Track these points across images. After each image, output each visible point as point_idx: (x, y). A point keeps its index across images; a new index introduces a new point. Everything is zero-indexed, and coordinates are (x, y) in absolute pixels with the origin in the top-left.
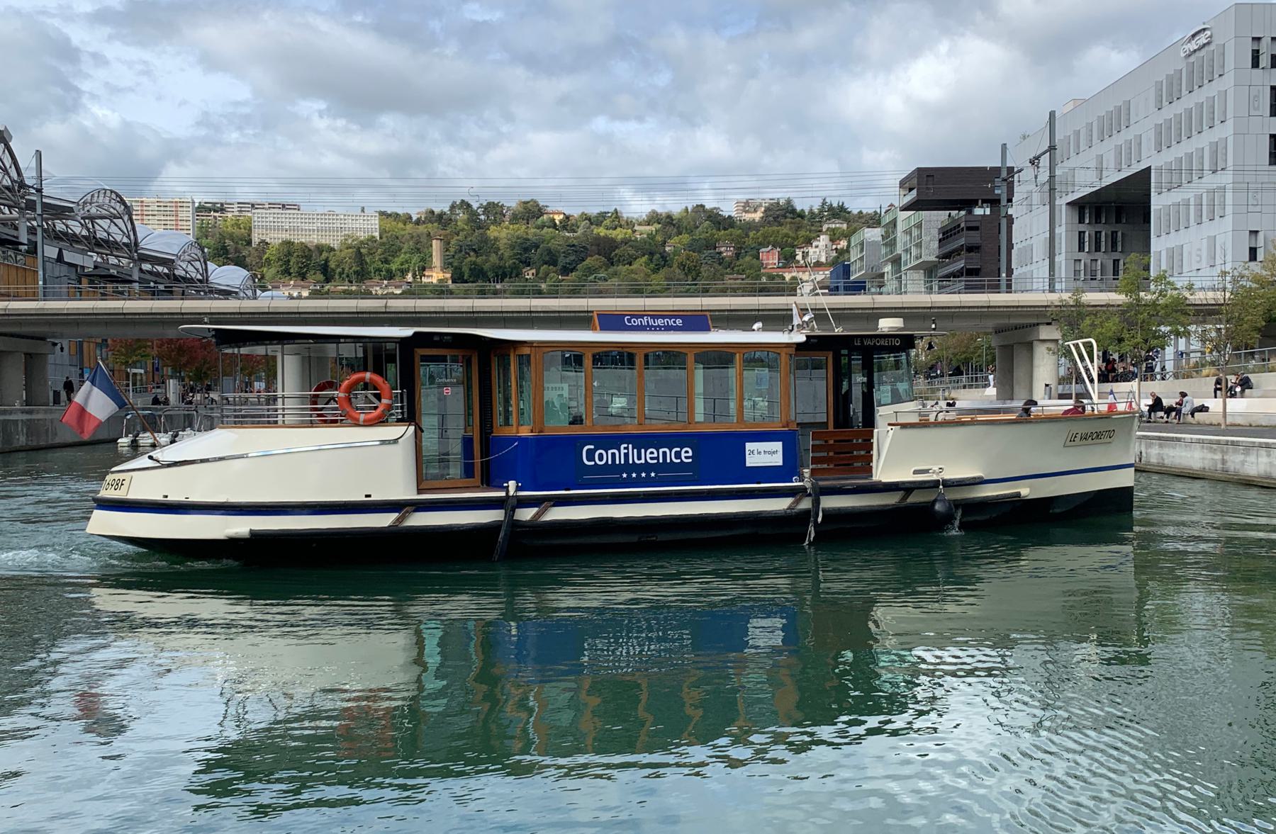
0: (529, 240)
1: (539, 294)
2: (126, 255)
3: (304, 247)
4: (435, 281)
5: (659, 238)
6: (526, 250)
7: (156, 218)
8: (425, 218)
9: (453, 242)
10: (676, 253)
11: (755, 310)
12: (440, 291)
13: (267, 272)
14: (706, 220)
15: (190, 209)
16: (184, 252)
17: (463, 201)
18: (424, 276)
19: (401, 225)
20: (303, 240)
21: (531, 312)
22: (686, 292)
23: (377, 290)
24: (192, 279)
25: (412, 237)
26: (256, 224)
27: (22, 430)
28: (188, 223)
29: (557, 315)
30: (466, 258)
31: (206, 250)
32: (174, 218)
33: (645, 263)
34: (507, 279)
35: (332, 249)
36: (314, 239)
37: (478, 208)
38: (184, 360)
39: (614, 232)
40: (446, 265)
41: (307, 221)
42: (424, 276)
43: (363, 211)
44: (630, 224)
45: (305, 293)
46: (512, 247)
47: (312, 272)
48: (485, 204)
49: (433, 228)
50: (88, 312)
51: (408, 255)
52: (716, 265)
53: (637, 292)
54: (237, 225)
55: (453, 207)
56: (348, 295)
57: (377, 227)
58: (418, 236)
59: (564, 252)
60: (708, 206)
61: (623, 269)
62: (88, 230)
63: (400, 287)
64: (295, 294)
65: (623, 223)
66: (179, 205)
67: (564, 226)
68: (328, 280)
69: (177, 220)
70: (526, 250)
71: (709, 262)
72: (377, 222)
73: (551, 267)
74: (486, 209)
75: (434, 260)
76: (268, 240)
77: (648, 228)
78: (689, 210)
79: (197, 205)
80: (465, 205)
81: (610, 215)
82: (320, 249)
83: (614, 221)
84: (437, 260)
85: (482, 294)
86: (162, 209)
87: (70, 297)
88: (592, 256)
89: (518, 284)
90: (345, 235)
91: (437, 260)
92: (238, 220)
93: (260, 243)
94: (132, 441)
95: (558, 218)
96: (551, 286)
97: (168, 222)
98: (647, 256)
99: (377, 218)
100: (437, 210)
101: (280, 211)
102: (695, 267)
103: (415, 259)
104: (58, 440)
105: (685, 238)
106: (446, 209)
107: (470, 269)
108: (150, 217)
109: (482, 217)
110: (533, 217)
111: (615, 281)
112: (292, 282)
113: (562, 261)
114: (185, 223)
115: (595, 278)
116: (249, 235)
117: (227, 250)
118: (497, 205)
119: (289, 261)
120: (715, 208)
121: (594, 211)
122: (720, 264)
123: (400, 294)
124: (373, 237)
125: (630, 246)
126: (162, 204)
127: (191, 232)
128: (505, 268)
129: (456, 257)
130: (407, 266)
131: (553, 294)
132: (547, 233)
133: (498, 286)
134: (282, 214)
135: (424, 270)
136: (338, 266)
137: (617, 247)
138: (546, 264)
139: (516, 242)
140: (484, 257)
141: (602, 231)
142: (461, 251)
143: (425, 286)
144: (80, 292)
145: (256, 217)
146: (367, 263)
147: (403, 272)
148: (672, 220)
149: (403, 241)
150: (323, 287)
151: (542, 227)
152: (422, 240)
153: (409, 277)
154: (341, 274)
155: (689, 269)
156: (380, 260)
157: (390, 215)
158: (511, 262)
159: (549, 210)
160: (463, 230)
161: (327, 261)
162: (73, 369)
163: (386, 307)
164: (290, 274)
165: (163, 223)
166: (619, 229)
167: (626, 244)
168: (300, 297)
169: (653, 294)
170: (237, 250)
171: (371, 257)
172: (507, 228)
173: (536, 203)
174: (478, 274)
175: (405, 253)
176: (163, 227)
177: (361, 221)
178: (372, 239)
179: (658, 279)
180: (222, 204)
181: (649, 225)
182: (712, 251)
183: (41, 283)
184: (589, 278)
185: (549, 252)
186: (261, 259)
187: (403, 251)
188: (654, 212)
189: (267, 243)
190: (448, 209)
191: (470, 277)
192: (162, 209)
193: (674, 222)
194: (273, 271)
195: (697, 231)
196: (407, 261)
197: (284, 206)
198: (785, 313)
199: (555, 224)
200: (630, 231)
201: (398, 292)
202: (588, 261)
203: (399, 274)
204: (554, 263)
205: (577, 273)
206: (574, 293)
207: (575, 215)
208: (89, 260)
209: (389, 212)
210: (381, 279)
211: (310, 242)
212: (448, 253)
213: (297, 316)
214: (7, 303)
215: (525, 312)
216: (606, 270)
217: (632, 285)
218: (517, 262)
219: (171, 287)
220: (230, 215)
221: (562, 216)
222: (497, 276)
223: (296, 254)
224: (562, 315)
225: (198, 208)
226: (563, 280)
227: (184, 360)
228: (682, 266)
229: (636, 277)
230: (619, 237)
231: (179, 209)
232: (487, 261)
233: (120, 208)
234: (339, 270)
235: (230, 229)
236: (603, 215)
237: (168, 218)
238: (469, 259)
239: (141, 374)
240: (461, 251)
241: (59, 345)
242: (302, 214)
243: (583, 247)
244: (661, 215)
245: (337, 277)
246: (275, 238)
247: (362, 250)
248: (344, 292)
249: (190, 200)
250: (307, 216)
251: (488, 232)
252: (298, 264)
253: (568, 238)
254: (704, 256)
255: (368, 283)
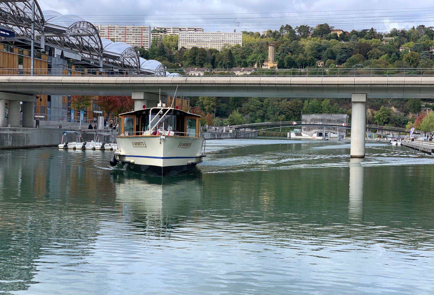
0: (321, 46)
1: (325, 74)
2: (97, 54)
3: (203, 50)
4: (269, 68)
5: (396, 44)
6: (319, 51)
7: (132, 36)
8: (267, 35)
9: (280, 47)
10: (406, 52)
11: (386, 84)
12: (272, 73)
13: (184, 63)
14: (425, 34)
15: (149, 31)
16: (125, 53)
17: (287, 25)
18: (263, 65)
19: (253, 39)
20: (203, 47)
21: (260, 84)
22: (409, 74)
23: (238, 73)
24: (132, 66)
25: (259, 45)
26: (180, 39)
27: (10, 138)
28: (147, 38)
29: (274, 86)
30: (285, 56)
31: (138, 52)
32: (140, 36)
33: (386, 58)
34: (307, 67)
35: (217, 51)
36: (209, 46)
37: (295, 29)
38: (110, 107)
39: (370, 41)
40: (276, 59)
41: (206, 37)
42: (263, 65)
43: (235, 32)
44: (380, 36)
45: (202, 74)
46: (312, 49)
47: (206, 63)
48: (299, 27)
49: (269, 40)
50: (46, 82)
51: (256, 54)
52: (429, 60)
53: (380, 73)
54: (171, 39)
55: (282, 29)
56: (222, 75)
57: (241, 39)
58: (262, 44)
59: (340, 52)
60: (427, 26)
61: (372, 61)
62: (79, 42)
63: (250, 70)
64: (197, 74)
65: (376, 36)
66: (143, 29)
67: (342, 38)
68: (214, 67)
69: (142, 37)
70: (319, 51)
71: (425, 57)
72: (241, 37)
73: (332, 60)
74: (299, 29)
75: (269, 57)
76: (186, 47)
77: (390, 38)
78: (415, 28)
79: (152, 29)
80: (288, 27)
81: (369, 31)
82: (212, 51)
83: (371, 34)
84: (271, 57)
85: (294, 74)
86: (135, 31)
87: (64, 74)
88: (356, 54)
89: (313, 69)
90: (225, 44)
91: (271, 57)
92: (172, 37)
93: (181, 48)
94: (65, 146)
95: (339, 33)
96: (332, 70)
97: (138, 38)
98: (387, 54)
99: (241, 35)
100: (273, 30)
101: (194, 32)
102: (416, 60)
103: (260, 56)
104: (30, 144)
105: (412, 44)
106: (278, 30)
107: (288, 62)
108: (129, 36)
109: (297, 34)
110: (325, 33)
111: (367, 68)
112: (196, 68)
113: (338, 57)
114: (146, 38)
115: (356, 66)
116: (177, 44)
117: (165, 52)
118: (306, 27)
119: (195, 57)
120: (431, 27)
121: (359, 28)
122: (431, 59)
123: (249, 74)
124: (239, 45)
125: (379, 49)
126: (135, 29)
127: (148, 43)
128: (307, 61)
129: (281, 55)
130: (255, 60)
131: (333, 74)
132: (332, 42)
133: (303, 70)
134: (194, 33)
135: (264, 62)
136: (219, 60)
137: (371, 49)
138: (329, 58)
139: (314, 47)
140: (296, 55)
141: (363, 40)
142: (284, 52)
143: (263, 70)
144: (71, 72)
145: (181, 35)
146: (234, 59)
147: (253, 64)
148: (405, 34)
149: (254, 46)
150: (211, 70)
151: (329, 39)
152: (264, 46)
153: (256, 66)
154: (221, 64)
155: (412, 61)
156: (241, 57)
157: (249, 33)
158: (310, 57)
159: (334, 29)
160: (286, 40)
161: (214, 57)
162: (64, 110)
163: (186, 81)
164: (195, 64)
165: (135, 38)
166: (373, 39)
167: (376, 47)
168: (199, 76)
169: (391, 74)
170: (171, 52)
171: (237, 55)
172: (310, 39)
173: (327, 25)
174: (292, 64)
175: (255, 53)
176: (135, 40)
177: (233, 37)
178: (238, 46)
179: (391, 67)
180: (165, 29)
181: (391, 37)
182: (427, 51)
183: (32, 67)
184: (353, 66)
185: (332, 52)
186: (182, 56)
187: (254, 52)
188: (395, 29)
189: (185, 49)
190: (279, 29)
191: (287, 65)
192: (135, 31)
193: (406, 35)
194: (187, 62)
195: (419, 40)
196: (255, 58)
197: (195, 29)
198: (403, 86)
199: (337, 37)
200: (379, 40)
201: (249, 73)
202: (353, 57)
203: (251, 64)
204: (334, 58)
205: (347, 63)
206: (344, 74)
207: (349, 32)
208: (78, 57)
209: (248, 32)
210: (241, 67)
211: (207, 48)
212: (277, 53)
213: (143, 85)
214: (9, 77)
215: (257, 84)
216: (363, 62)
217: (378, 70)
218: (313, 57)
219: (122, 70)
220: (168, 34)
221: (341, 32)
222: (302, 65)
223: (199, 54)
224: (277, 86)
225: (153, 31)
226: (338, 67)
227: (110, 107)
228: (408, 59)
229: (380, 65)
230: (373, 43)
231: (143, 31)
232: (297, 57)
233: (92, 31)
234: (220, 62)
235: (168, 42)
236: (364, 31)
237: (138, 36)
238: (287, 56)
239: (101, 114)
240: (284, 52)
241: (39, 98)
242: (203, 33)
243: (351, 49)
244: (399, 31)
245: (219, 65)
246: (189, 46)
247: (232, 52)
248: (221, 74)
249: (148, 27)
250: (206, 35)
251: (299, 41)
252: (200, 58)
253: (343, 44)
254: (422, 54)
255: (234, 69)
